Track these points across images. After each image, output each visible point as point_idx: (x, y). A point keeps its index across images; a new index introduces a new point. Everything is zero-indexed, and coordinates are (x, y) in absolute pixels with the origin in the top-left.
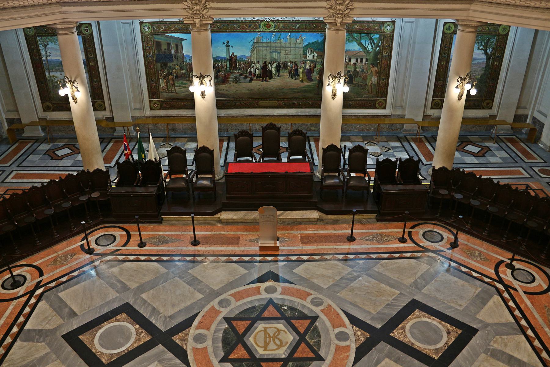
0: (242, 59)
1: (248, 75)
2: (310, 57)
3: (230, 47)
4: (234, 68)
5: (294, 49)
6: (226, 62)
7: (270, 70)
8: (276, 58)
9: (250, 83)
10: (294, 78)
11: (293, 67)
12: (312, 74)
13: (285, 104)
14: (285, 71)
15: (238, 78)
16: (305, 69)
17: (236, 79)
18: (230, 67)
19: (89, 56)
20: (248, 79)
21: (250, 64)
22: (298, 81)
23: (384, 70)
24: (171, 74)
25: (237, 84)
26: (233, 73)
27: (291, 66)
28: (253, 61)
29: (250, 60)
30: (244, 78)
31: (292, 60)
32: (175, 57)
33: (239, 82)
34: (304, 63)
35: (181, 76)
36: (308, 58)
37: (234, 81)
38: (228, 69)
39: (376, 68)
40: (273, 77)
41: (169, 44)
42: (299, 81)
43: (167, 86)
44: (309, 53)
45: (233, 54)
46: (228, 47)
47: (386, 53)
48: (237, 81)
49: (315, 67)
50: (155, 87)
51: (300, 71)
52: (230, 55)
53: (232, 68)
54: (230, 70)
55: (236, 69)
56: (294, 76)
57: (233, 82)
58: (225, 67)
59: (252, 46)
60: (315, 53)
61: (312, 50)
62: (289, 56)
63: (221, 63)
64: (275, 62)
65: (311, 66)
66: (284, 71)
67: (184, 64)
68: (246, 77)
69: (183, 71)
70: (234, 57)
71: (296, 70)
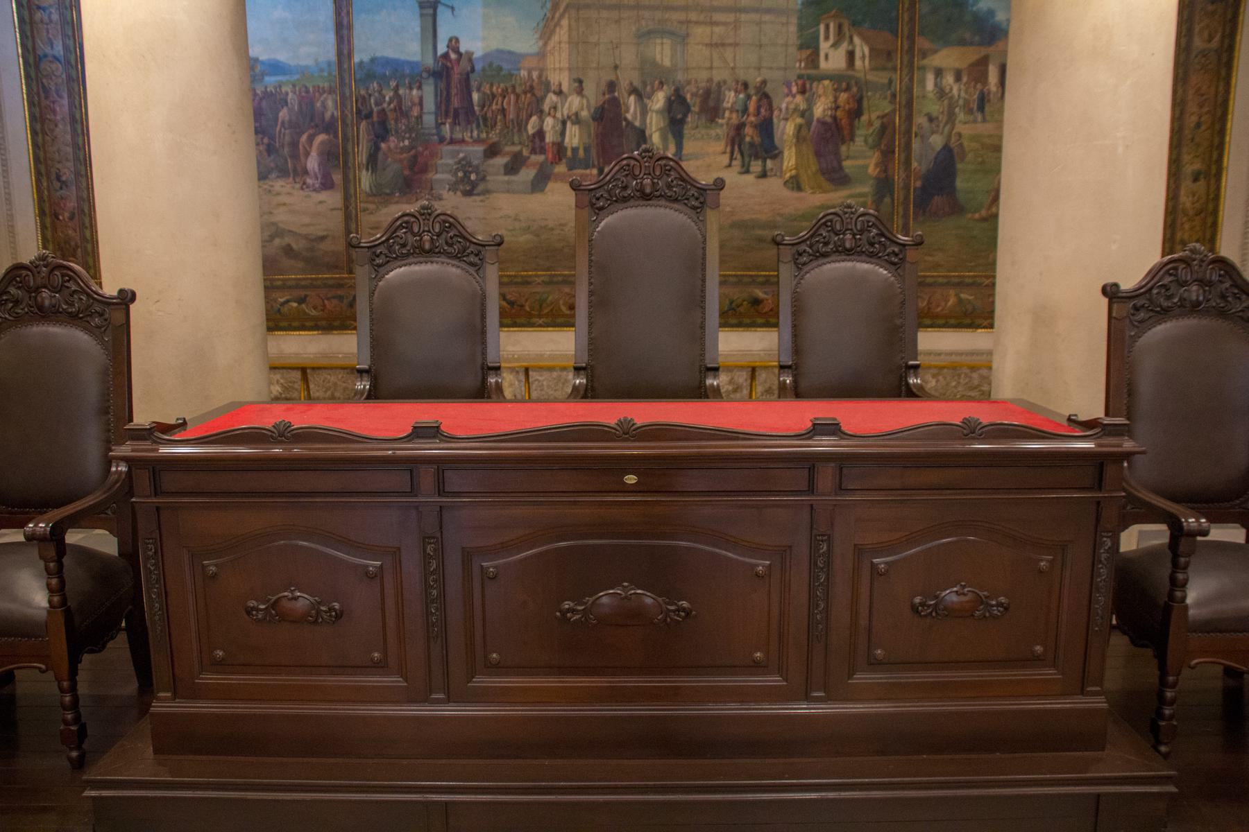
0: (500, 69)
1: (525, 153)
2: (833, 59)
3: (440, 9)
4: (456, 115)
5: (755, 17)
6: (420, 88)
7: (637, 124)
8: (667, 62)
9: (538, 196)
10: (756, 166)
12: (844, 148)
14: (713, 133)
16: (809, 123)
17: (466, 173)
18: (437, 114)
20: (527, 174)
22: (774, 185)
23: (1198, 125)
26: (452, 142)
27: (739, 107)
28: (554, 78)
29: (535, 75)
30: (506, 166)
31: (742, 76)
33: (481, 187)
34: (803, 91)
36: (823, 65)
37: (456, 183)
38: (429, 120)
44: (827, 38)
47: (1210, 39)
48: (474, 185)
49: (856, 113)
50: (72, 218)
51: (786, 130)
52: (442, 48)
53: (447, 115)
54: (439, 125)
55: (469, 122)
56: (757, 157)
57: (453, 188)
58: (415, 112)
60: (857, 40)
61: (840, 27)
62: (729, 53)
63: (397, 86)
64: (662, 84)
65: (837, 108)
66: (703, 131)
68: (513, 167)
70: (458, 60)
71: (766, 128)
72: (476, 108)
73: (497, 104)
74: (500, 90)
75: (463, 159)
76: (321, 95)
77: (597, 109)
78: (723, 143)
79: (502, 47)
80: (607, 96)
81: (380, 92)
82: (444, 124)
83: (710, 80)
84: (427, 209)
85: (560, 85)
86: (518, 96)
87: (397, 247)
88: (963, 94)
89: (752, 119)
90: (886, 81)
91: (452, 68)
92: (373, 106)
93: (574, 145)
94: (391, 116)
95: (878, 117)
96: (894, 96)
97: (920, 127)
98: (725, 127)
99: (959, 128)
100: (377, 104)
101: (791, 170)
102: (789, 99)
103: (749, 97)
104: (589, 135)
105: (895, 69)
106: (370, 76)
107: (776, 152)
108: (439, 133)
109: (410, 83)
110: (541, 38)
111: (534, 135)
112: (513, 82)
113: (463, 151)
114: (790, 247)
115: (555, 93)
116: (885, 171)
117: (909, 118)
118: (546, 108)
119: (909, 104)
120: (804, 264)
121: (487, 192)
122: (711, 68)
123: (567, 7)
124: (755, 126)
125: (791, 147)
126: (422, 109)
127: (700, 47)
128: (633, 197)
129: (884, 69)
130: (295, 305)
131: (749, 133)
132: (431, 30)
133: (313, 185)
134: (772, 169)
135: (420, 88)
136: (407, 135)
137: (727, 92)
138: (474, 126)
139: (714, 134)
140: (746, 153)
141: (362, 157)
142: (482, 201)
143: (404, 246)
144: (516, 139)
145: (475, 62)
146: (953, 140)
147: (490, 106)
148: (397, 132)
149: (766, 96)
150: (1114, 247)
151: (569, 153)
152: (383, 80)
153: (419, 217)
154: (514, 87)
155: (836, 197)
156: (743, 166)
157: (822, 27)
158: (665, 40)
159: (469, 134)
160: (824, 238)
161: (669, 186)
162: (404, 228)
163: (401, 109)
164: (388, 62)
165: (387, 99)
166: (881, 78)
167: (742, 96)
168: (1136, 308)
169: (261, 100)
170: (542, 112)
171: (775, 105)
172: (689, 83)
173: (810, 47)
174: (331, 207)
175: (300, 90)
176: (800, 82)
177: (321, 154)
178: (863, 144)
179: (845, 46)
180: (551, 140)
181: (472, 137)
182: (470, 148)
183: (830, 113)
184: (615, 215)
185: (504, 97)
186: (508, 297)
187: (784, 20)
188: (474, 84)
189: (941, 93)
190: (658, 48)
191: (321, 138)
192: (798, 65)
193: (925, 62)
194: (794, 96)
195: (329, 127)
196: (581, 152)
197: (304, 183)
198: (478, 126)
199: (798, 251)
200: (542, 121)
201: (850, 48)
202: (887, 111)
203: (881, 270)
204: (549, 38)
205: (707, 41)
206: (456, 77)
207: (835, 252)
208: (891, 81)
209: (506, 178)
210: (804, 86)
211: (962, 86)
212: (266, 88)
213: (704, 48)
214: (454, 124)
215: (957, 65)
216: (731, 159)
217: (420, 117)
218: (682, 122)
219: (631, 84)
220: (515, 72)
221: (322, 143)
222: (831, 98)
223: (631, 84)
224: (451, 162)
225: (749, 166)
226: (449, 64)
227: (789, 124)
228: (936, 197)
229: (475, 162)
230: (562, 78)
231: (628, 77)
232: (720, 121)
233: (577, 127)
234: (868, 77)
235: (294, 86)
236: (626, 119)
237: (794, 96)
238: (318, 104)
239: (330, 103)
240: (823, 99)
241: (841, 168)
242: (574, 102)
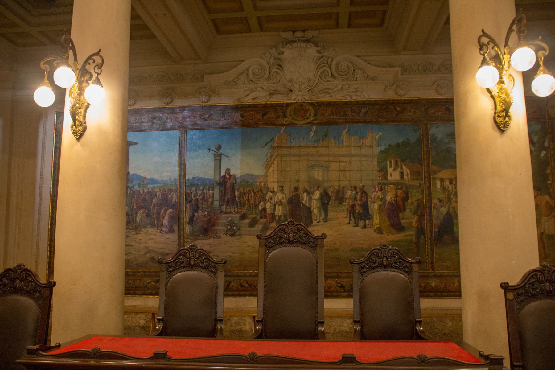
0: (247, 182)
1: (258, 218)
2: (394, 176)
3: (223, 157)
4: (228, 202)
5: (359, 158)
6: (213, 190)
7: (307, 205)
8: (320, 179)
10: (361, 223)
11: (358, 197)
12: (401, 215)
13: (342, 287)
14: (341, 208)
22: (370, 231)
25: (233, 238)
26: (226, 213)
27: (353, 197)
28: (271, 186)
29: (263, 184)
30: (249, 223)
31: (354, 184)
33: (238, 233)
34: (381, 190)
38: (216, 203)
39: (547, 198)
40: (315, 223)
42: (373, 230)
44: (391, 167)
45: (228, 171)
46: (218, 157)
48: (235, 232)
51: (374, 207)
52: (223, 173)
53: (224, 202)
54: (220, 206)
55: (233, 204)
56: (361, 220)
57: (226, 233)
58: (210, 200)
59: (269, 155)
60: (404, 167)
61: (396, 162)
62: (347, 174)
63: (203, 189)
64: (318, 188)
68: (253, 224)
70: (230, 178)
71: (365, 206)
72: (237, 198)
73: (246, 197)
74: (247, 191)
75: (231, 220)
76: (171, 193)
77: (290, 199)
78: (346, 213)
79: (248, 173)
80: (294, 193)
81: (196, 191)
82: (223, 205)
83: (339, 186)
84: (193, 247)
85: (273, 188)
86: (255, 193)
87: (179, 264)
90: (418, 185)
91: (227, 182)
92: (193, 197)
93: (279, 215)
94: (200, 201)
95: (416, 200)
96: (423, 191)
97: (435, 204)
98: (346, 206)
100: (194, 197)
101: (377, 225)
102: (375, 193)
103: (357, 193)
104: (286, 210)
105: (422, 179)
106: (192, 185)
107: (370, 216)
108: (220, 210)
109: (209, 188)
110: (265, 169)
111: (262, 210)
112: (253, 188)
113: (230, 217)
114: (358, 265)
115: (271, 192)
116: (421, 224)
117: (430, 201)
118: (267, 199)
119: (430, 194)
120: (364, 272)
121: (241, 235)
122: (340, 181)
123: (277, 155)
124: (360, 205)
125: (376, 215)
126: (213, 199)
127: (335, 172)
128: (284, 242)
129: (417, 179)
130: (154, 283)
131: (358, 209)
133: (165, 231)
134: (368, 224)
135: (213, 190)
136: (207, 210)
137: (347, 191)
138: (236, 206)
139: (342, 209)
140: (356, 218)
141: (187, 219)
142: (238, 239)
143: (182, 263)
144: (254, 212)
145: (236, 179)
146: (451, 210)
147: (243, 197)
148: (202, 209)
149: (365, 192)
150: (514, 262)
151: (277, 218)
153: (190, 250)
154: (253, 189)
155: (398, 236)
156: (355, 223)
157: (388, 162)
158: (319, 169)
159: (233, 210)
160: (373, 260)
161: (301, 237)
162: (183, 255)
163: (204, 199)
164: (200, 179)
165: (199, 194)
166: (416, 183)
167: (354, 192)
168: (519, 295)
169: (146, 194)
170: (265, 200)
171: (369, 195)
172: (330, 187)
174: (172, 240)
175: (162, 190)
176: (380, 186)
177: (169, 218)
178: (409, 212)
179: (399, 170)
180: (269, 212)
181: (234, 211)
182: (233, 216)
183: (394, 199)
184: (277, 250)
185: (249, 194)
186: (249, 282)
187: (371, 159)
188: (236, 188)
189: (444, 189)
190: (316, 173)
191: (170, 210)
192: (378, 178)
193: (435, 176)
194: (377, 192)
195: (173, 206)
196: (282, 218)
197: (161, 230)
198: (237, 206)
199: (361, 267)
201: (401, 171)
202: (419, 198)
203: (401, 275)
204: (269, 169)
205: (338, 169)
207: (379, 267)
208: (420, 185)
209: (249, 229)
210: (382, 187)
211: (453, 186)
212: (148, 189)
213: (336, 172)
214: (227, 205)
215: (450, 177)
216: (350, 220)
217: (212, 202)
218: (327, 204)
219: (305, 188)
220: (254, 183)
221: (170, 213)
222: (394, 193)
223: (305, 188)
224: (225, 222)
225: (358, 223)
226: (226, 180)
227: (375, 204)
228: (445, 236)
229: (236, 222)
231: (303, 185)
232: (344, 203)
233: (281, 206)
234: (410, 183)
235: (160, 189)
236: (302, 203)
237: (377, 192)
239: (174, 196)
240: (390, 193)
241: (400, 223)
242: (280, 196)
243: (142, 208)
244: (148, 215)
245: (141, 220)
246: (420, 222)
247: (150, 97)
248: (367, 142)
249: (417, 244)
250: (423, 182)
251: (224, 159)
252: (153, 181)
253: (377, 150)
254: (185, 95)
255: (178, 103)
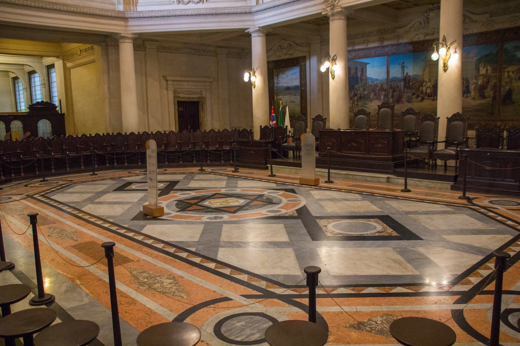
1: (420, 94)
2: (483, 71)
15: (411, 98)
16: (477, 85)
19: (302, 81)
20: (420, 99)
21: (421, 83)
24: (356, 95)
25: (409, 103)
26: (406, 93)
29: (422, 79)
32: (360, 79)
34: (476, 79)
35: (364, 97)
38: (402, 88)
41: (357, 69)
43: (352, 106)
45: (407, 74)
46: (403, 67)
48: (410, 101)
49: (488, 83)
51: (472, 87)
52: (405, 75)
54: (404, 90)
57: (406, 101)
58: (400, 87)
60: (489, 67)
61: (485, 64)
65: (484, 82)
67: (366, 85)
68: (418, 97)
69: (366, 92)
88: (514, 77)
89: (465, 85)
99: (513, 84)
117: (501, 83)
121: (412, 102)
123: (428, 65)
132: (403, 72)
141: (391, 95)
146: (512, 87)
152: (395, 81)
166: (494, 74)
173: (478, 69)
179: (486, 68)
189: (509, 76)
195: (385, 90)
196: (430, 94)
200: (423, 88)
206: (408, 79)
217: (401, 88)
230: (427, 79)
238: (383, 86)
239: (385, 86)
240: (480, 80)
242: (429, 84)
243: (373, 92)
244: (375, 95)
245: (373, 97)
246: (494, 94)
247: (374, 42)
248: (470, 56)
249: (492, 104)
250: (498, 74)
251: (405, 68)
252: (377, 80)
253: (476, 58)
254: (389, 39)
255: (386, 43)
